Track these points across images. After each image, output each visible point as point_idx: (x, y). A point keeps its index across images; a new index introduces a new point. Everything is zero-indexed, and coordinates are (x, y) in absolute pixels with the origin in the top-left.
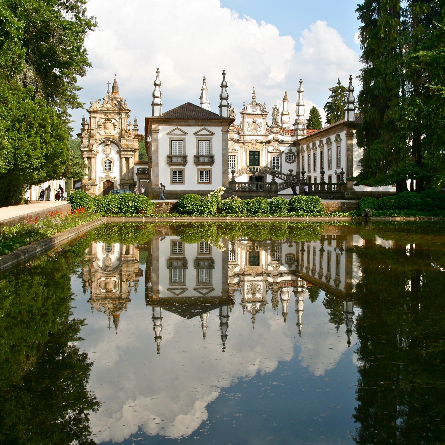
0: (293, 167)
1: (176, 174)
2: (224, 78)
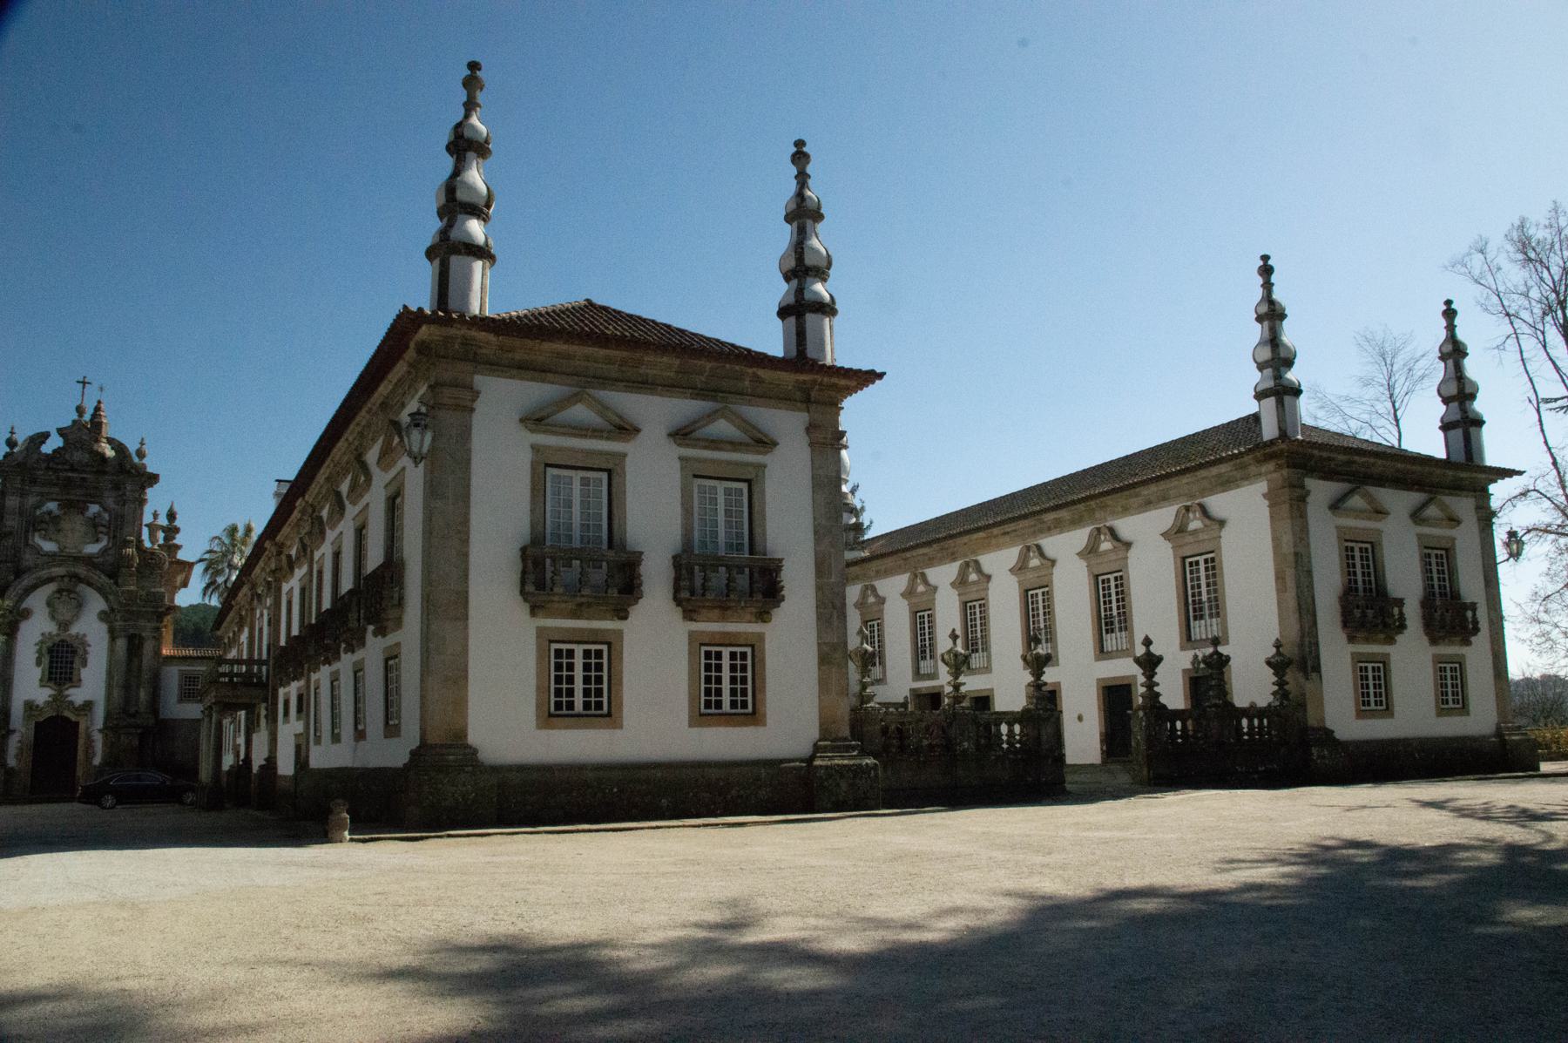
1: (571, 667)
2: (802, 178)
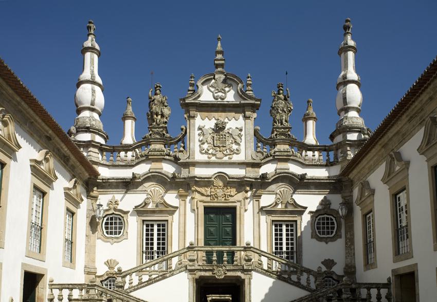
0: (335, 250)
